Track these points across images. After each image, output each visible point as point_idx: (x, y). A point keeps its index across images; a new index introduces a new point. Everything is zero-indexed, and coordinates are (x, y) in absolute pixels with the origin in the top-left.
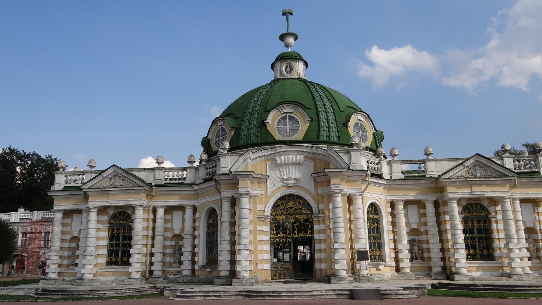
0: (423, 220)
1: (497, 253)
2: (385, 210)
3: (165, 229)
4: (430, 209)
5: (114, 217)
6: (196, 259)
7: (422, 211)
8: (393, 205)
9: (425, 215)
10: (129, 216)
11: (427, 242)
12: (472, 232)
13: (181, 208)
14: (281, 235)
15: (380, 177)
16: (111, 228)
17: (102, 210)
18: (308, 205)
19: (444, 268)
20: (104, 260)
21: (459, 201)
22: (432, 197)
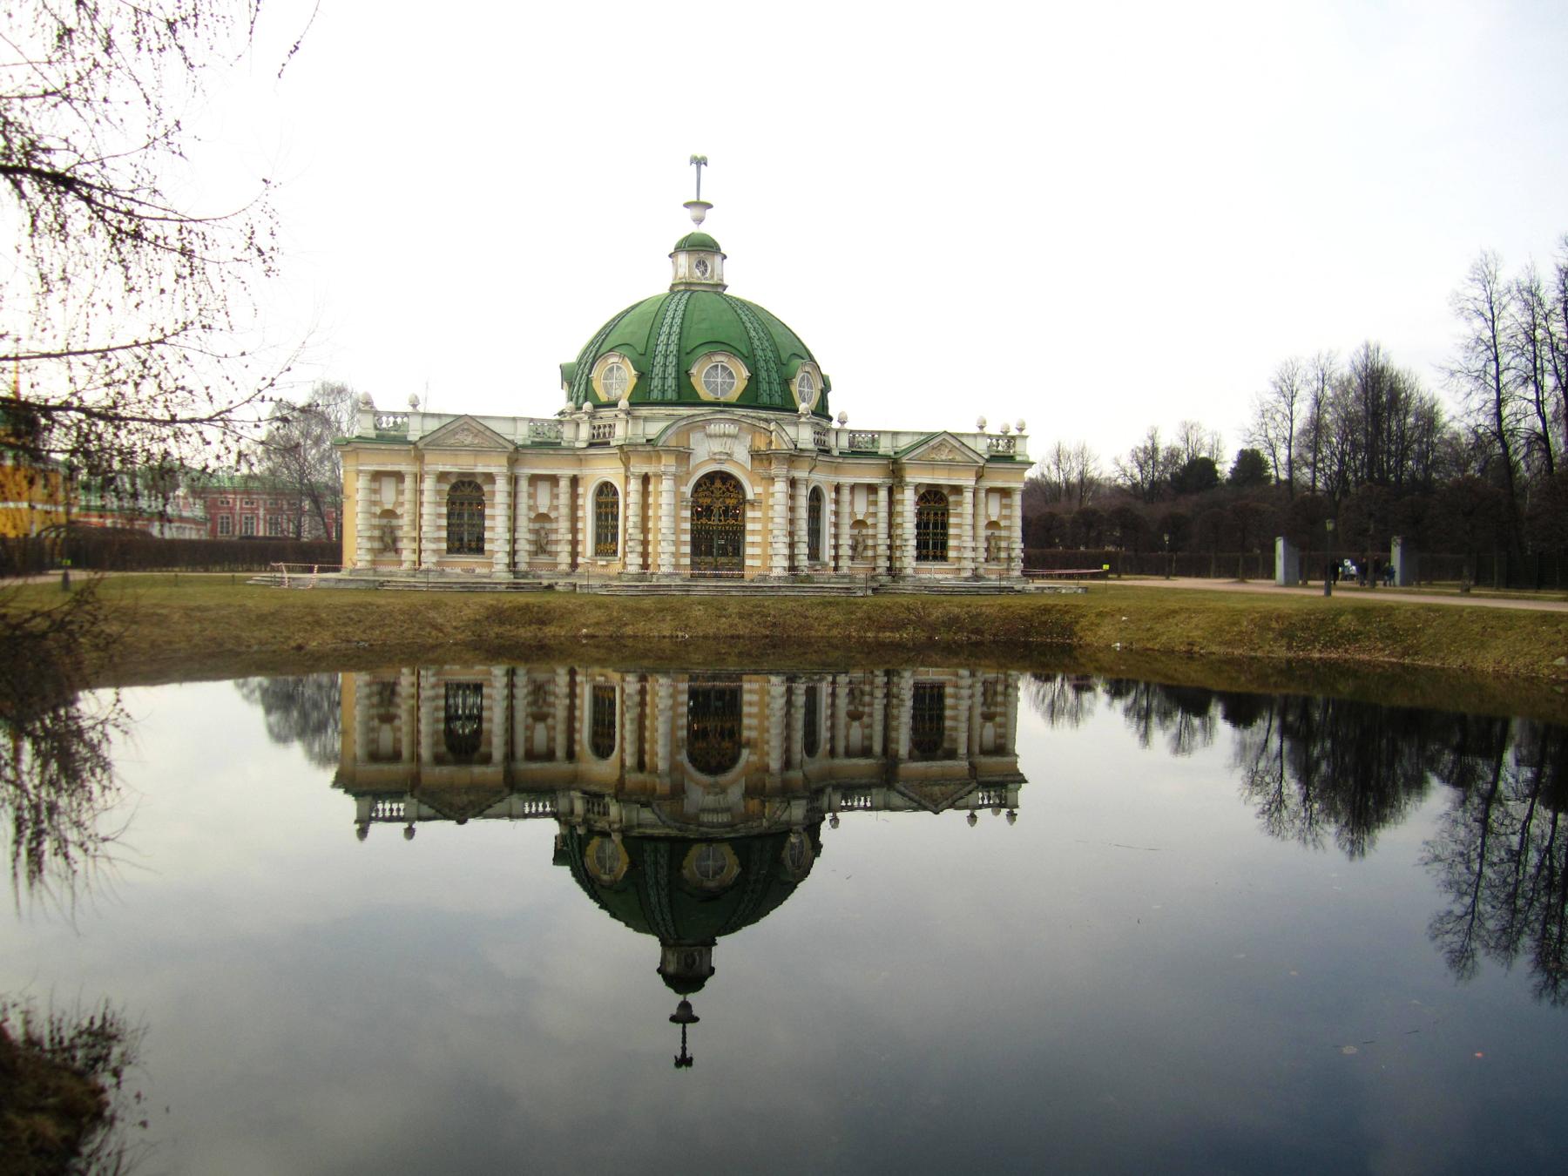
0: (872, 509)
1: (952, 554)
2: (828, 496)
3: (530, 508)
4: (883, 495)
5: (454, 488)
6: (580, 549)
7: (872, 498)
8: (838, 489)
9: (875, 503)
10: (479, 488)
11: (874, 536)
12: (927, 526)
13: (554, 480)
14: (704, 521)
15: (827, 452)
16: (451, 503)
17: (442, 477)
18: (739, 486)
19: (889, 569)
20: (444, 546)
21: (917, 487)
22: (889, 481)
